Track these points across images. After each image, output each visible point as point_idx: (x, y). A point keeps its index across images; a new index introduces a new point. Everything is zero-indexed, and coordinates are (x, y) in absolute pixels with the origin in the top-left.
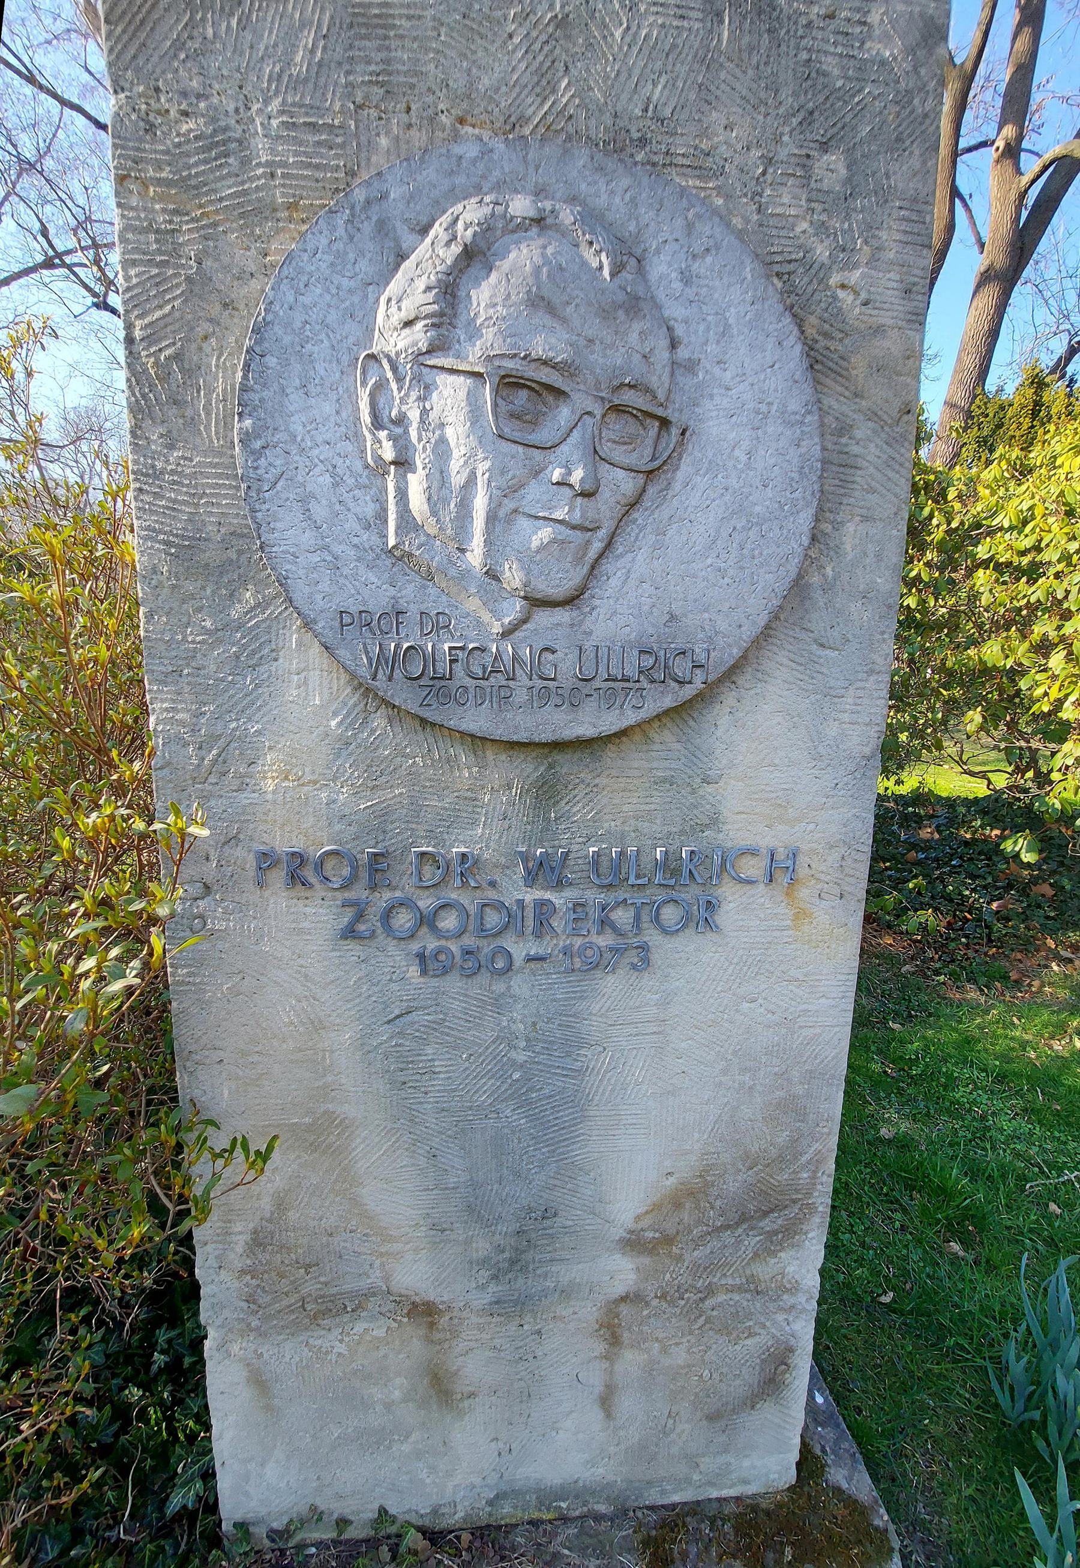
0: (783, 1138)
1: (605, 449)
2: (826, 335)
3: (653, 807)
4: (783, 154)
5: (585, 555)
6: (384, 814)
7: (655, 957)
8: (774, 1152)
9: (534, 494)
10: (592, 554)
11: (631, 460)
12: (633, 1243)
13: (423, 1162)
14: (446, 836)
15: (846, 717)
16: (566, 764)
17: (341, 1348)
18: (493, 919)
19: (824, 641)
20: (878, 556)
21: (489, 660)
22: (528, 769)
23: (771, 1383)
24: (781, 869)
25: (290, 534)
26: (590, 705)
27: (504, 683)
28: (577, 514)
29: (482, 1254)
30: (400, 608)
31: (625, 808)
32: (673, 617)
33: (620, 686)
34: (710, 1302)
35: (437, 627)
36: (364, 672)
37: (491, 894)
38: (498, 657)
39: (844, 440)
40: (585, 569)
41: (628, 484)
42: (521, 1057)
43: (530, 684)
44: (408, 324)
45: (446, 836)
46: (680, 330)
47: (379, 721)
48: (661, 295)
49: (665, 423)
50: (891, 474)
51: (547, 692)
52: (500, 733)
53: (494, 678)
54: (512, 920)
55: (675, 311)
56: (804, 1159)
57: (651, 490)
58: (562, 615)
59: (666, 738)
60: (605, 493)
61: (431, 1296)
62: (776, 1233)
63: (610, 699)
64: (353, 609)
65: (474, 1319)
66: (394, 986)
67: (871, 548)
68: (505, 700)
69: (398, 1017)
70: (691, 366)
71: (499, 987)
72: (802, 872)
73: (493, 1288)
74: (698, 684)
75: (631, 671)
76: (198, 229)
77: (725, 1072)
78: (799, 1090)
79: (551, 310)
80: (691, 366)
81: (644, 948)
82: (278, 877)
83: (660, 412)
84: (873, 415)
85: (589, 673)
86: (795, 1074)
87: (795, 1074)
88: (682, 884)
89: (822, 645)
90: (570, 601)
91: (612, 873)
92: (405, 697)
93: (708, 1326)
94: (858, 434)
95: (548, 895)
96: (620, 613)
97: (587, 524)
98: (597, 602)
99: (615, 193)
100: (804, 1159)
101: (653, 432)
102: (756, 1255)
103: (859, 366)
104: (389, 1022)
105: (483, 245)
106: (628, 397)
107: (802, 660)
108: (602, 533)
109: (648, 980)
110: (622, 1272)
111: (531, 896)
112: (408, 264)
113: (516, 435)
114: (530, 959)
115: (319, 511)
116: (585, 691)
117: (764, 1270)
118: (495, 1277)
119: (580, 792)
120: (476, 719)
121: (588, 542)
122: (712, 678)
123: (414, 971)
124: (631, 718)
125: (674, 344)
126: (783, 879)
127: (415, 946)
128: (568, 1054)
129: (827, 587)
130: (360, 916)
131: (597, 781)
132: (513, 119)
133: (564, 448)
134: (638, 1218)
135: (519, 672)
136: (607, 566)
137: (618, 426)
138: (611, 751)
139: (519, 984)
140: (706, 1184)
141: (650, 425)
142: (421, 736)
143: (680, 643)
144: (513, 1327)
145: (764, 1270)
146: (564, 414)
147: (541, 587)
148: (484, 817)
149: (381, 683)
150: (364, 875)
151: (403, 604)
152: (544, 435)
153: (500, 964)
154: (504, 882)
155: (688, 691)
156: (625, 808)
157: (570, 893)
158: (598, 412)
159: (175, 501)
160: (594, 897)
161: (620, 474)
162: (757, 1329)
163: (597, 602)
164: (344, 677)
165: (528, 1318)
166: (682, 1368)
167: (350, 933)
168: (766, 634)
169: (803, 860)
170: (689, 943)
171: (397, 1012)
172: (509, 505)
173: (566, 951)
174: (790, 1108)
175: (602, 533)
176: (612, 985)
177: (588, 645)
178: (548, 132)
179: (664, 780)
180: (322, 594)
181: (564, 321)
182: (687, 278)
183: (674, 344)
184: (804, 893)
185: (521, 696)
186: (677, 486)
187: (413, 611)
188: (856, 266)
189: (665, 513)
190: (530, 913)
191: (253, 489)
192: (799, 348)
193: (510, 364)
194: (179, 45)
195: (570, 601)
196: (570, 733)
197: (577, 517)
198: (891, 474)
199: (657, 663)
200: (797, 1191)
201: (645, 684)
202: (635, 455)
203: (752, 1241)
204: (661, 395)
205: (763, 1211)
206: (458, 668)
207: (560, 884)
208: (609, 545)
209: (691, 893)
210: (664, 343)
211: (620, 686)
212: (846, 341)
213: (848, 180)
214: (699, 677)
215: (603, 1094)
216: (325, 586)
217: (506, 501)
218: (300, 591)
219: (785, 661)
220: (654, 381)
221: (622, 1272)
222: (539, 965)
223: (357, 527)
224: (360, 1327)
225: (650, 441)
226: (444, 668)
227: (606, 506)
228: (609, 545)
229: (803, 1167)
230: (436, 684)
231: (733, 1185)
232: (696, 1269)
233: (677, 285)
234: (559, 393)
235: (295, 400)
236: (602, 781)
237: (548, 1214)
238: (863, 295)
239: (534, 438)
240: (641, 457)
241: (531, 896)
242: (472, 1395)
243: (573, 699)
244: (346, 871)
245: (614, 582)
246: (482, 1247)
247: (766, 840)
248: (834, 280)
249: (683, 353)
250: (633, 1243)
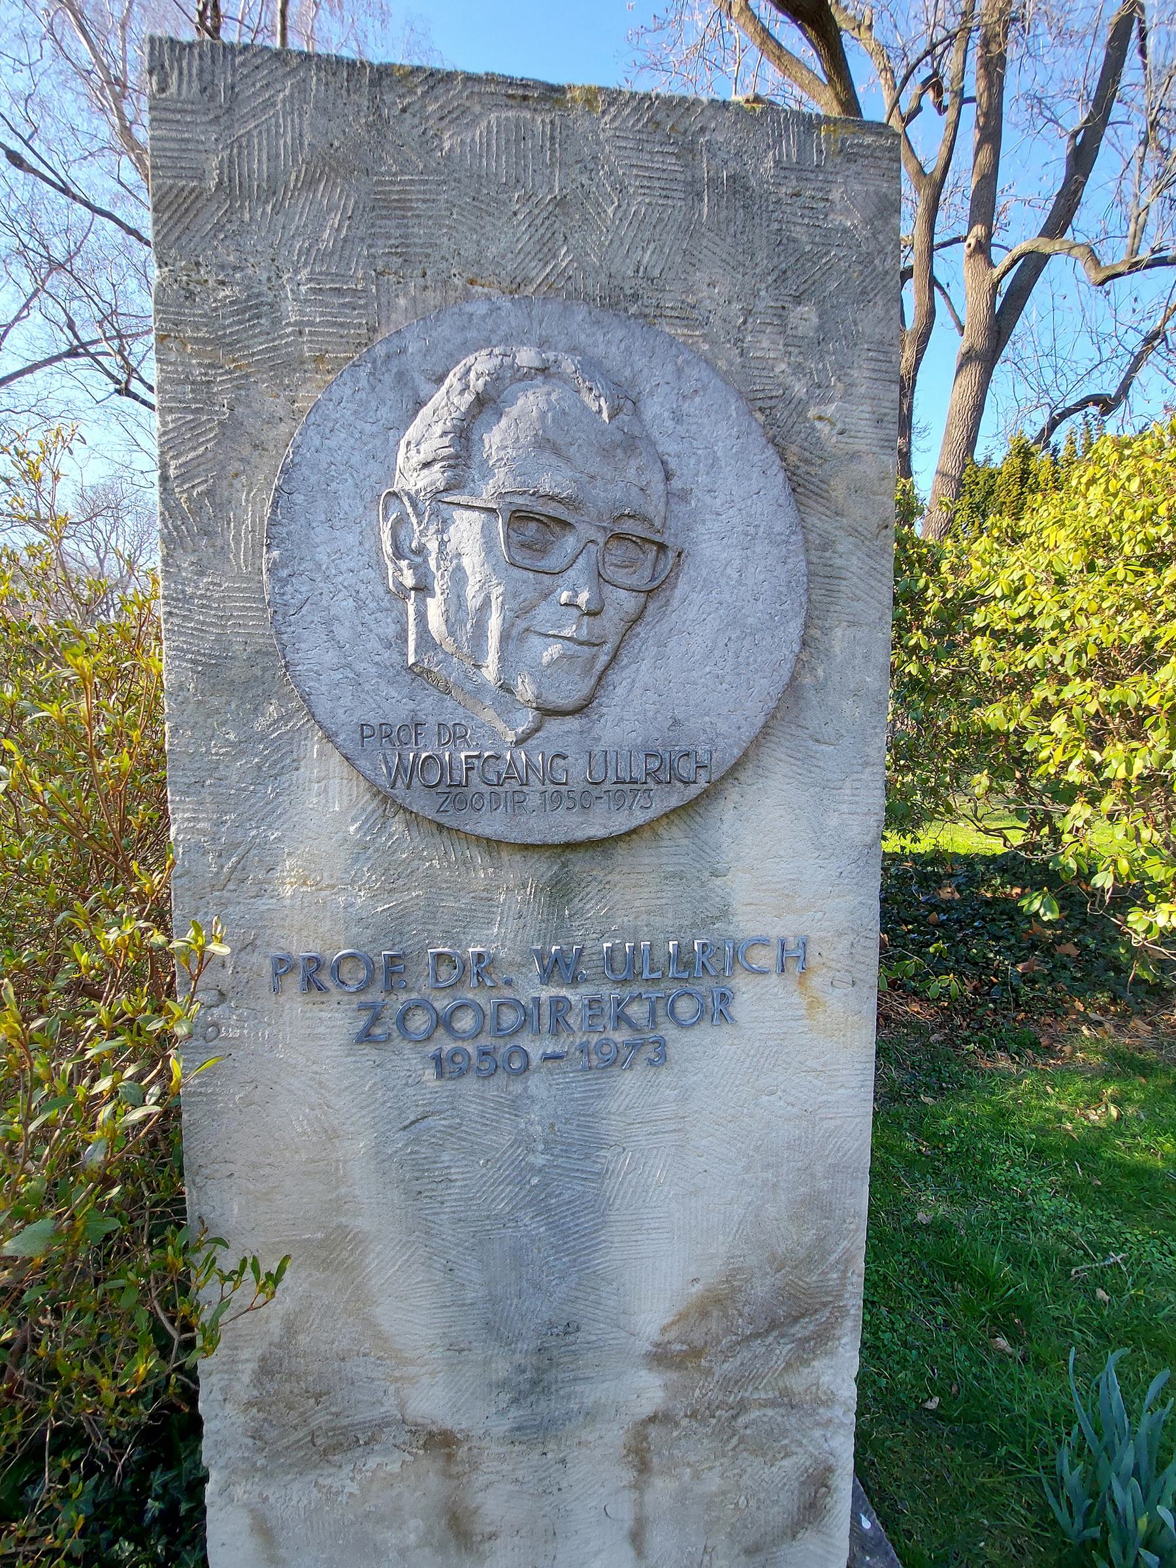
0: (809, 1237)
1: (609, 572)
2: (807, 462)
3: (664, 901)
4: (761, 306)
5: (592, 668)
6: (400, 917)
7: (671, 1051)
8: (802, 1253)
9: (544, 612)
10: (599, 666)
11: (633, 581)
12: (660, 1357)
13: (439, 1277)
14: (462, 936)
15: (844, 808)
16: (579, 864)
17: (352, 1488)
18: (509, 1018)
19: (819, 736)
20: (866, 657)
22: (543, 868)
23: (811, 1510)
24: (792, 958)
25: (314, 655)
26: (600, 807)
27: (518, 788)
28: (584, 631)
29: (502, 1375)
30: (418, 720)
31: (637, 903)
32: (676, 722)
34: (741, 1420)
35: (454, 737)
36: (383, 781)
37: (508, 993)
38: (512, 763)
39: (827, 554)
40: (593, 681)
41: (629, 602)
42: (540, 1160)
43: (543, 788)
44: (427, 465)
45: (462, 936)
46: (673, 464)
47: (397, 826)
48: (655, 434)
49: (662, 547)
50: (873, 583)
51: (560, 796)
52: (514, 836)
53: (507, 785)
54: (528, 1017)
55: (668, 447)
56: (832, 1258)
57: (651, 607)
58: (572, 723)
59: (676, 836)
60: (610, 611)
61: (449, 1424)
62: (807, 1340)
63: (619, 800)
64: (374, 722)
65: (496, 1449)
66: (410, 1091)
67: (860, 651)
68: (518, 803)
69: (413, 1123)
70: (684, 496)
71: (517, 1088)
72: (813, 961)
73: (514, 1412)
74: (703, 784)
75: (637, 773)
76: (231, 380)
77: (747, 1169)
78: (824, 1185)
79: (556, 451)
80: (684, 496)
81: (660, 1043)
82: (293, 982)
84: (854, 532)
85: (599, 776)
86: (819, 1169)
87: (819, 1169)
88: (693, 977)
89: (817, 741)
90: (578, 710)
91: (627, 967)
93: (742, 1446)
94: (841, 548)
95: (563, 992)
96: (628, 719)
97: (594, 640)
98: (605, 710)
99: (610, 343)
100: (832, 1258)
102: (789, 1365)
103: (838, 489)
104: (405, 1128)
105: (493, 393)
106: (628, 526)
107: (800, 756)
108: (607, 648)
109: (665, 1076)
110: (648, 1390)
111: (547, 993)
112: (426, 411)
113: (527, 563)
114: (547, 1058)
115: (343, 633)
116: (595, 794)
117: (798, 1382)
118: (515, 1401)
119: (593, 888)
120: (491, 824)
121: (594, 657)
122: (714, 777)
123: (430, 1074)
124: (640, 817)
125: (668, 477)
126: (794, 968)
127: (431, 1049)
128: (587, 1156)
129: (820, 687)
130: (376, 1019)
131: (609, 878)
132: (518, 280)
133: (571, 573)
134: (664, 1330)
135: (532, 778)
136: (613, 677)
137: (619, 552)
138: (622, 849)
139: (536, 1084)
140: (735, 1290)
141: (647, 552)
142: (438, 840)
143: (684, 746)
144: (535, 1456)
145: (798, 1382)
146: (570, 542)
147: (551, 698)
148: (500, 917)
149: (400, 790)
150: (380, 977)
151: (421, 717)
152: (552, 561)
153: (516, 1064)
154: (519, 980)
155: (693, 791)
156: (637, 903)
157: (585, 990)
158: (601, 541)
159: (203, 623)
160: (610, 992)
162: (794, 1448)
163: (605, 710)
164: (364, 785)
165: (552, 1446)
166: (716, 1495)
167: (365, 1037)
168: (766, 731)
169: (813, 949)
170: (705, 1036)
171: (412, 1118)
172: (522, 625)
173: (584, 1049)
174: (815, 1205)
175: (607, 648)
176: (629, 1083)
177: (597, 750)
178: (550, 289)
179: (674, 875)
180: (346, 711)
181: (568, 460)
182: (678, 418)
183: (668, 477)
184: (816, 982)
185: (534, 800)
186: (675, 603)
187: (432, 722)
188: (831, 400)
189: (665, 627)
190: (546, 1011)
191: (280, 614)
192: (781, 475)
193: (520, 500)
194: (219, 227)
195: (578, 710)
196: (580, 835)
197: (584, 634)
198: (873, 583)
199: (663, 766)
200: (827, 1294)
202: (635, 576)
203: (784, 1350)
204: (658, 523)
205: (791, 1316)
206: (474, 774)
207: (575, 981)
208: (615, 657)
209: (705, 985)
210: (659, 476)
211: (627, 788)
212: (826, 466)
213: (820, 328)
214: (703, 776)
215: (624, 1197)
216: (347, 701)
217: (518, 621)
218: (323, 708)
219: (783, 757)
220: (650, 510)
221: (648, 1390)
222: (556, 1063)
223: (378, 646)
224: (372, 1463)
225: (649, 564)
226: (460, 775)
227: (611, 623)
228: (615, 657)
229: (832, 1267)
230: (453, 791)
231: (761, 1289)
232: (727, 1384)
233: (669, 424)
234: (565, 524)
235: (321, 532)
236: (614, 877)
237: (571, 1328)
238: (839, 426)
239: (543, 564)
240: (641, 578)
241: (547, 993)
242: (493, 1536)
243: (584, 802)
244: (362, 974)
245: (620, 691)
246: (501, 1369)
247: (775, 931)
248: (812, 413)
249: (676, 484)
250: (660, 1357)
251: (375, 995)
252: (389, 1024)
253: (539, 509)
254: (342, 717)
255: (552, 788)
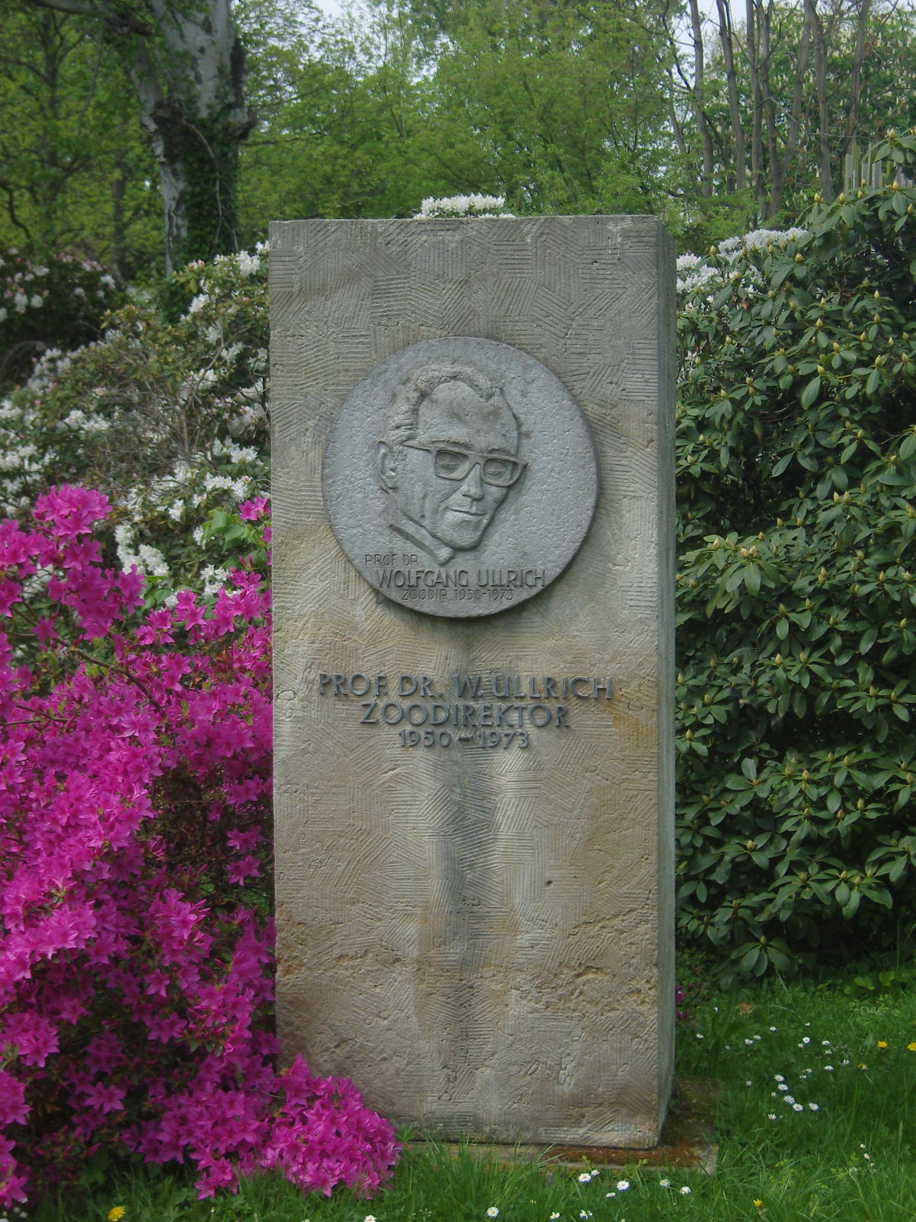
9: (457, 497)
10: (483, 526)
18: (442, 715)
21: (435, 577)
26: (485, 598)
32: (525, 554)
33: (498, 589)
38: (439, 576)
44: (398, 427)
46: (522, 417)
49: (515, 464)
52: (441, 613)
53: (440, 587)
58: (469, 556)
74: (540, 587)
75: (505, 582)
80: (527, 435)
83: (512, 459)
85: (484, 583)
90: (474, 547)
92: (395, 595)
93: (581, 998)
95: (472, 703)
96: (499, 554)
101: (510, 467)
105: (428, 390)
106: (494, 455)
114: (461, 740)
120: (429, 606)
121: (481, 521)
122: (547, 582)
127: (400, 729)
133: (467, 480)
136: (491, 530)
137: (492, 469)
143: (529, 567)
146: (466, 466)
149: (384, 590)
150: (375, 691)
151: (396, 551)
152: (456, 475)
153: (445, 742)
155: (535, 591)
158: (482, 462)
161: (494, 489)
162: (616, 1005)
164: (366, 586)
172: (444, 505)
175: (487, 517)
182: (524, 394)
186: (524, 492)
195: (474, 547)
197: (473, 510)
199: (519, 580)
201: (512, 587)
204: (513, 451)
207: (476, 698)
208: (492, 521)
211: (498, 589)
225: (508, 472)
226: (413, 582)
228: (492, 521)
234: (465, 457)
240: (505, 481)
241: (461, 703)
251: (371, 700)
252: (378, 715)
253: (451, 449)
254: (356, 551)
255: (460, 588)
